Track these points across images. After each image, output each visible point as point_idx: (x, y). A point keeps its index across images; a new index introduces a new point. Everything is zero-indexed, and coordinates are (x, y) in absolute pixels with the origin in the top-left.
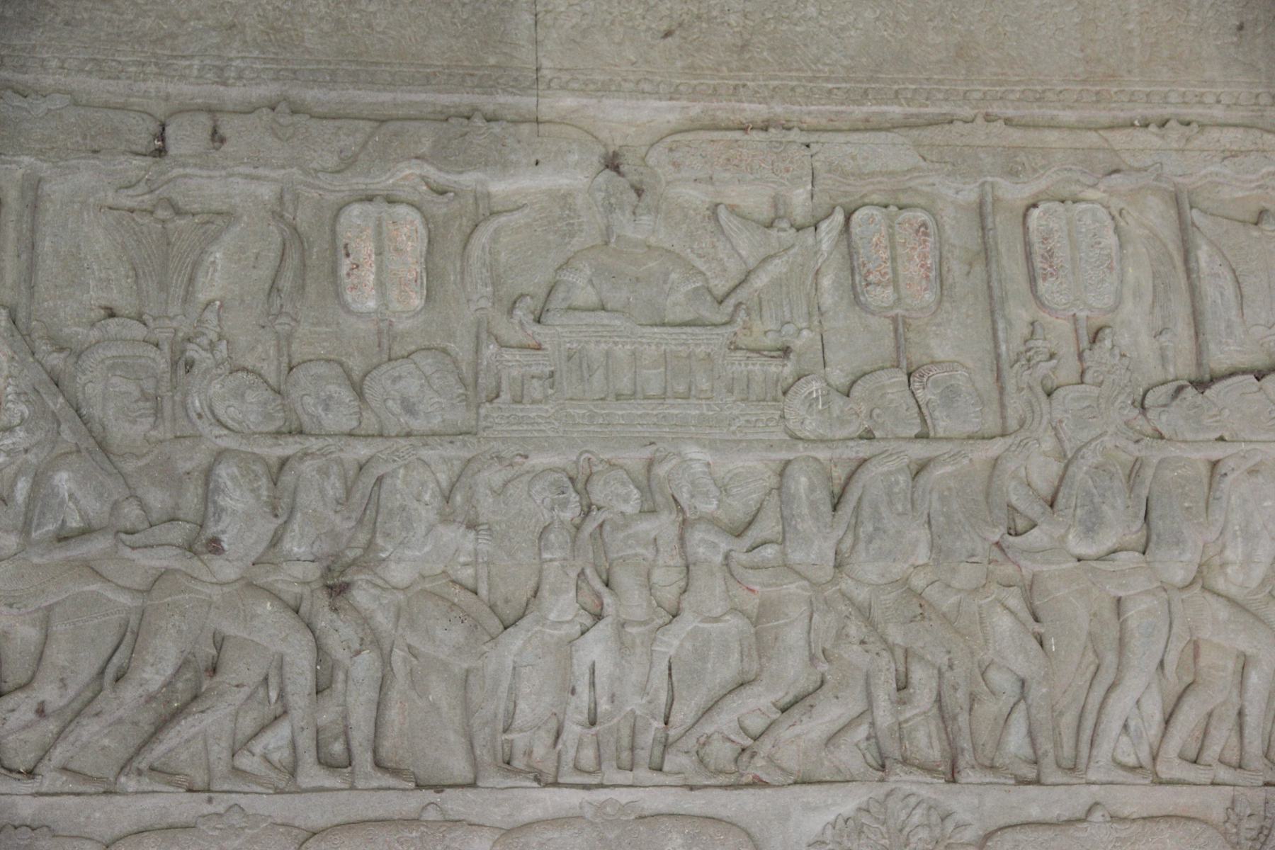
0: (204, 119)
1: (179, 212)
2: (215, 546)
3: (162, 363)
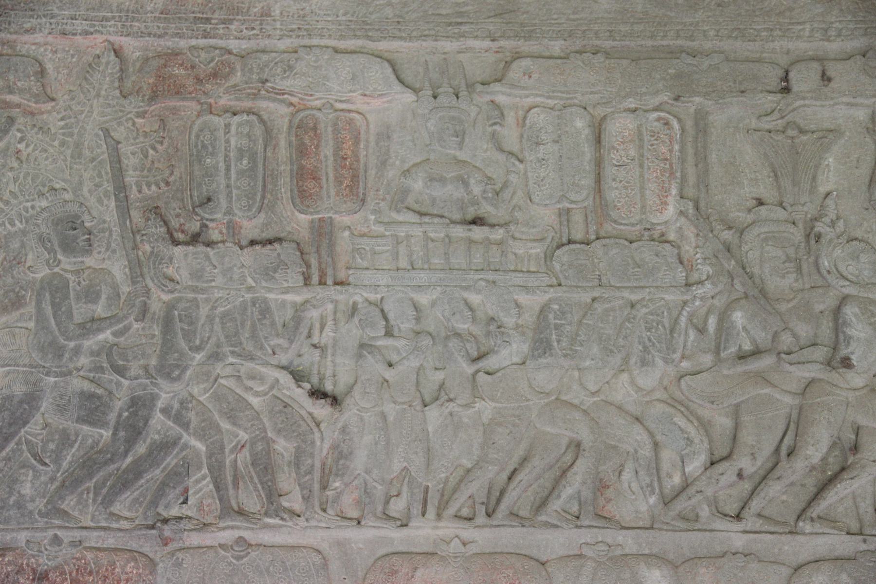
0: (815, 65)
1: (802, 131)
2: (846, 363)
3: (797, 234)
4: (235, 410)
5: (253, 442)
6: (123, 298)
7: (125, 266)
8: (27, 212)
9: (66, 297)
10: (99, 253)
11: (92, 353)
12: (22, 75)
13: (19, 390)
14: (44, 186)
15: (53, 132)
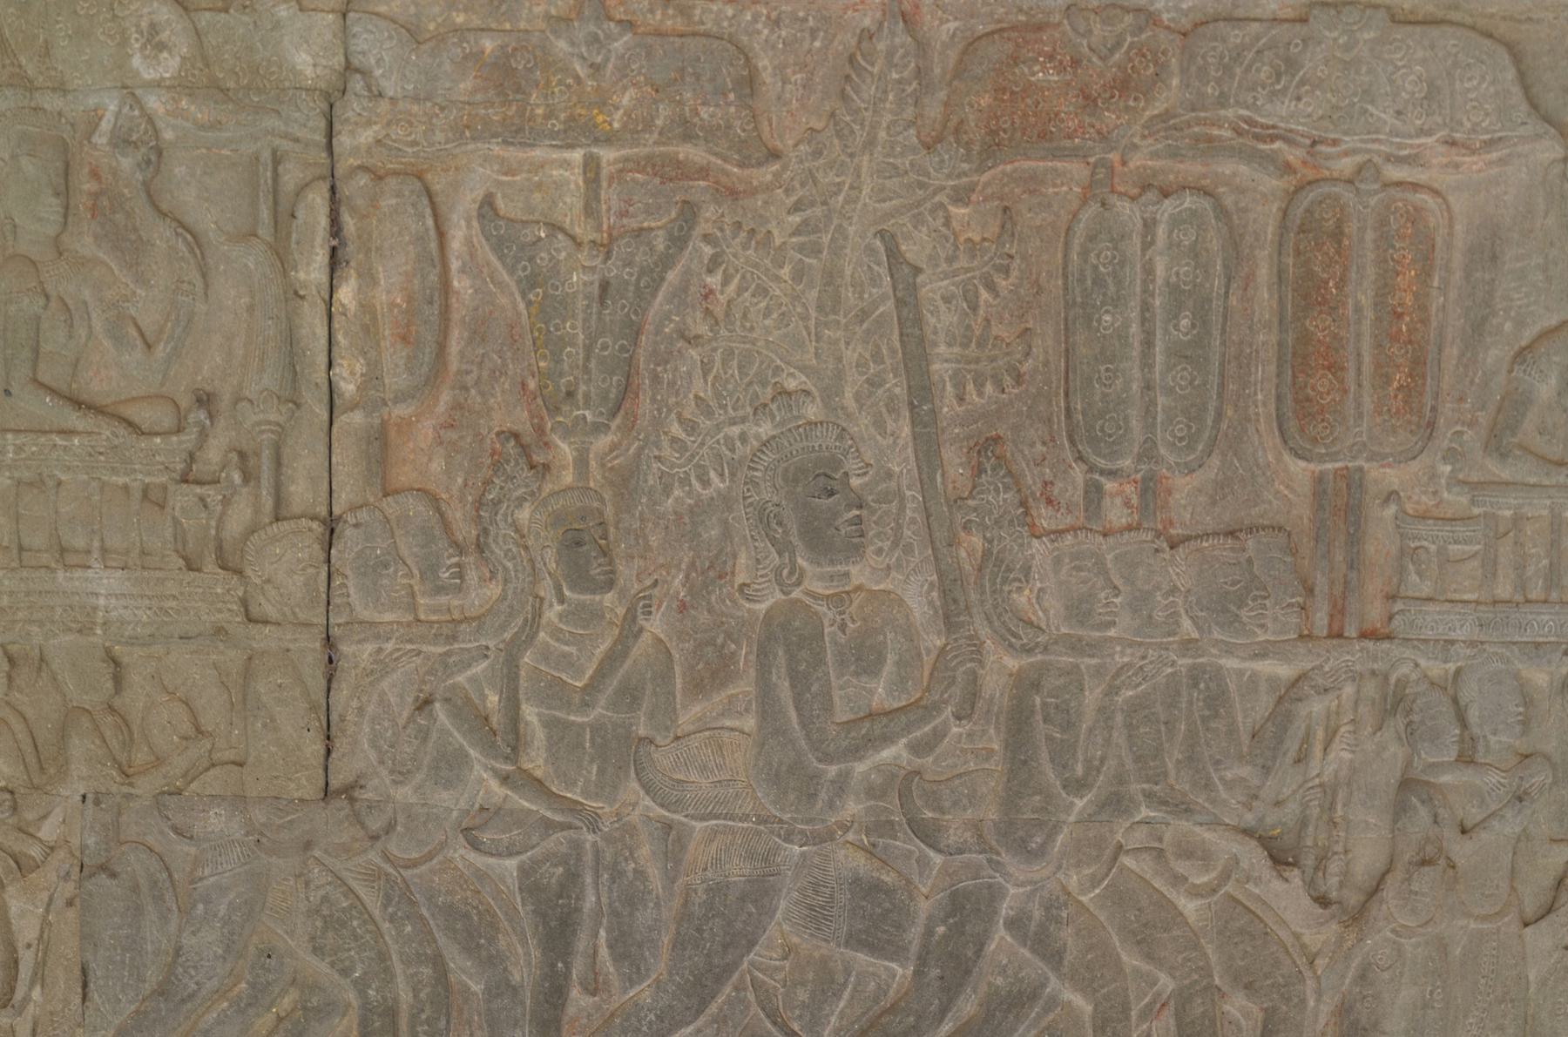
4: (1151, 926)
5: (1183, 999)
6: (928, 661)
7: (932, 584)
8: (733, 450)
9: (818, 660)
10: (879, 552)
11: (871, 792)
12: (708, 87)
13: (738, 871)
14: (764, 384)
15: (778, 242)
